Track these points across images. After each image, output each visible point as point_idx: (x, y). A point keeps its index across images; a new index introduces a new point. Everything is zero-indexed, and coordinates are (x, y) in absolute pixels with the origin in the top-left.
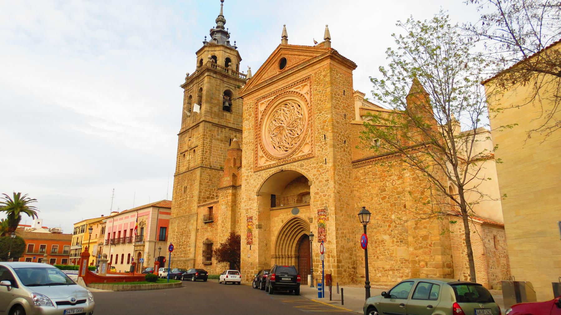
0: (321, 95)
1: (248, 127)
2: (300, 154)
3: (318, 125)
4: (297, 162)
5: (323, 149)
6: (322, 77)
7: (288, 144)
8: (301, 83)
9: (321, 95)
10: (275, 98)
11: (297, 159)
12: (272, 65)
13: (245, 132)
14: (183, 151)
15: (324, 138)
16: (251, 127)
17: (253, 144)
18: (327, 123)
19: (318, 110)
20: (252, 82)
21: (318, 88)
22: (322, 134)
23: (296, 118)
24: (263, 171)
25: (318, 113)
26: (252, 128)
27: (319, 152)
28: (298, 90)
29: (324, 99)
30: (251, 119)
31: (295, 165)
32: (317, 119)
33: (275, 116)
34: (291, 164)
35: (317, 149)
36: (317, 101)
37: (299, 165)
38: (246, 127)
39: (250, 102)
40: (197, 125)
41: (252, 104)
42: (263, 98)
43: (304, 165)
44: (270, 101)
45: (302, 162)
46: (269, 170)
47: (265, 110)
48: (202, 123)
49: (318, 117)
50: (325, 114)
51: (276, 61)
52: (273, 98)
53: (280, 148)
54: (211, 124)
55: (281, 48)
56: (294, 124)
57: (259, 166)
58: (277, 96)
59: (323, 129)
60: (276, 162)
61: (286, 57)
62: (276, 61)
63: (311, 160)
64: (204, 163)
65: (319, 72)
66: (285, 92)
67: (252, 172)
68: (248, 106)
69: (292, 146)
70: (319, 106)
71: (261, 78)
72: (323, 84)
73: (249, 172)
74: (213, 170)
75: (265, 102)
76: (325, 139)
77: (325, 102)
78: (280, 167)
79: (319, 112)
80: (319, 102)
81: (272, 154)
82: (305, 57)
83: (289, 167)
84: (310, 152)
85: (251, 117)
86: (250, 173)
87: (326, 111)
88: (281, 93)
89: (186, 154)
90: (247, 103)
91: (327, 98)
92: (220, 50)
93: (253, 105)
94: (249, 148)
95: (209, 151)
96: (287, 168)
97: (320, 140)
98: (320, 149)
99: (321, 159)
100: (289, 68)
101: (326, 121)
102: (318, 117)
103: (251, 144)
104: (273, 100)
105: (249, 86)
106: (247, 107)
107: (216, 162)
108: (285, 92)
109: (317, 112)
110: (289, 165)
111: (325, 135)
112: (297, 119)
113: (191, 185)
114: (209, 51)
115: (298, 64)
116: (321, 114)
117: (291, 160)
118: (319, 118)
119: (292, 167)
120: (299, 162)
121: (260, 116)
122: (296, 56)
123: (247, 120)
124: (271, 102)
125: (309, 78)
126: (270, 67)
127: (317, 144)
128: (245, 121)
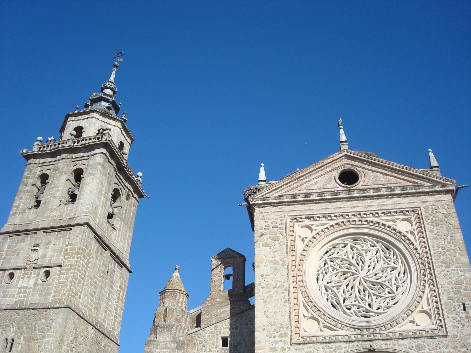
0: (445, 242)
1: (271, 259)
2: (410, 327)
3: (446, 285)
4: (409, 341)
5: (463, 325)
6: (442, 216)
7: (370, 305)
8: (395, 214)
9: (445, 242)
10: (337, 224)
11: (404, 334)
12: (326, 173)
13: (263, 265)
14: (13, 266)
15: (462, 307)
16: (277, 258)
17: (286, 290)
18: (464, 285)
19: (443, 262)
20: (279, 187)
21: (435, 230)
22: (458, 301)
23: (384, 266)
24: (320, 346)
25: (442, 266)
26: (281, 263)
27: (455, 329)
28: (391, 224)
29: (452, 248)
30: (277, 245)
31: (403, 345)
32: (442, 275)
33: (330, 253)
34: (392, 341)
35: (452, 324)
36: (436, 248)
37: (414, 345)
38: (264, 257)
39: (275, 217)
40: (67, 228)
41: (280, 222)
42: (306, 218)
43: (424, 346)
44: (326, 226)
45: (420, 341)
46: (337, 345)
47: (314, 237)
48: (82, 227)
49: (443, 273)
50: (459, 271)
51: (334, 169)
52: (333, 222)
53: (349, 309)
54: (94, 234)
55: (345, 155)
56: (380, 274)
57: (302, 333)
58: (343, 222)
59: (458, 292)
60: (352, 333)
61: (356, 169)
62: (334, 169)
63: (440, 339)
64: (74, 301)
65: (434, 207)
66: (360, 221)
67: (285, 343)
68: (269, 223)
69: (379, 311)
70: (445, 257)
71: (300, 186)
72: (445, 227)
73: (276, 342)
74: (82, 320)
75: (312, 225)
76: (465, 309)
77: (456, 253)
78: (367, 344)
79: (444, 265)
80: (440, 250)
81: (338, 318)
82: (400, 181)
83: (389, 347)
84: (434, 327)
85: (277, 243)
86: (281, 345)
87: (460, 267)
88: (351, 220)
89: (17, 273)
90: (268, 217)
91: (457, 247)
92: (117, 126)
93: (282, 224)
94: (274, 296)
95: (82, 281)
96: (384, 346)
97: (455, 310)
98: (456, 324)
99: (462, 342)
100: (365, 187)
101: (462, 281)
102: (443, 273)
103: (280, 289)
104: (332, 226)
105: (271, 191)
106: (266, 224)
107: (85, 306)
108: (360, 221)
109: (439, 264)
110: (388, 342)
111: (464, 305)
112: (387, 268)
113: (30, 339)
114: (98, 119)
115: (386, 186)
116: (449, 269)
117: (391, 334)
118: (446, 275)
119: (396, 347)
120: (414, 340)
121: (300, 246)
122: (381, 175)
123: (266, 245)
124: (327, 228)
125: (413, 211)
126: (322, 175)
127: (450, 316)
128: (261, 247)
